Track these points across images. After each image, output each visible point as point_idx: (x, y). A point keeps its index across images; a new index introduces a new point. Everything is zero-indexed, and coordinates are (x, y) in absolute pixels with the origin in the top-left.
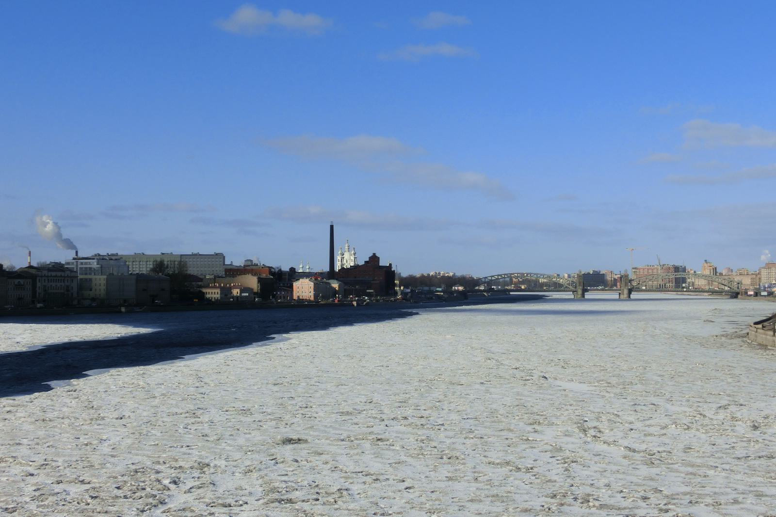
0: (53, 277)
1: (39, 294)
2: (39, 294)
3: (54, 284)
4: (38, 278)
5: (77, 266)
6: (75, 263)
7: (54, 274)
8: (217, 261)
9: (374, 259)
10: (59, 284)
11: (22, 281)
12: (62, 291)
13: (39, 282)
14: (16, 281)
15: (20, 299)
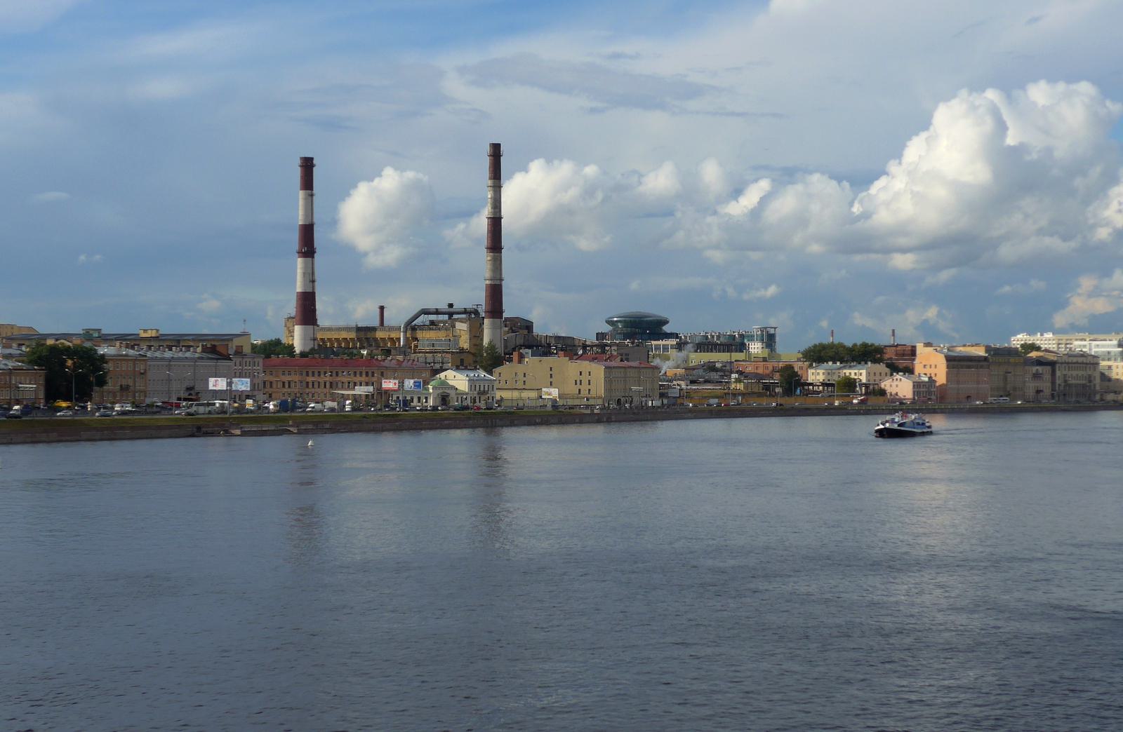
1: (1059, 385)
2: (1059, 385)
3: (1074, 373)
4: (1057, 366)
5: (1090, 349)
6: (1088, 347)
7: (1075, 360)
8: (1050, 344)
10: (1080, 373)
11: (1040, 369)
12: (1084, 382)
13: (1059, 370)
14: (1034, 369)
15: (1038, 392)
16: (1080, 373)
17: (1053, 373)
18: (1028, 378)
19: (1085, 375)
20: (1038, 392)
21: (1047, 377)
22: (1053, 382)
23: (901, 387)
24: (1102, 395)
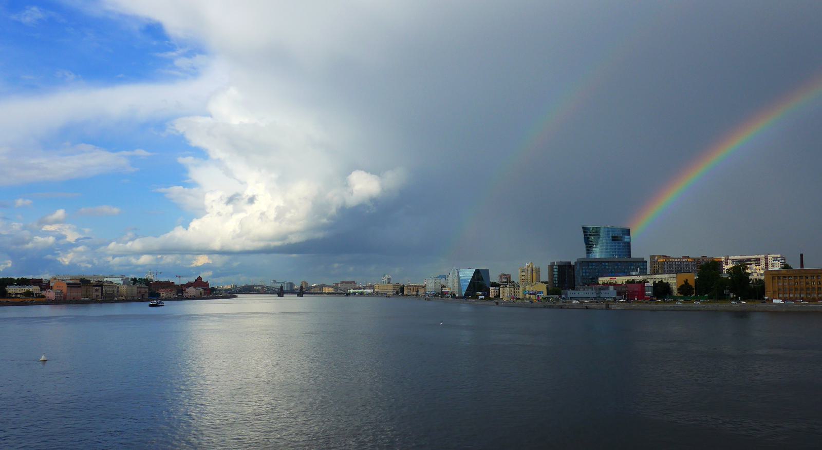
10: (111, 289)
14: (96, 288)
15: (97, 296)
16: (111, 289)
17: (102, 290)
18: (94, 290)
20: (97, 296)
21: (100, 291)
22: (102, 294)
23: (50, 294)
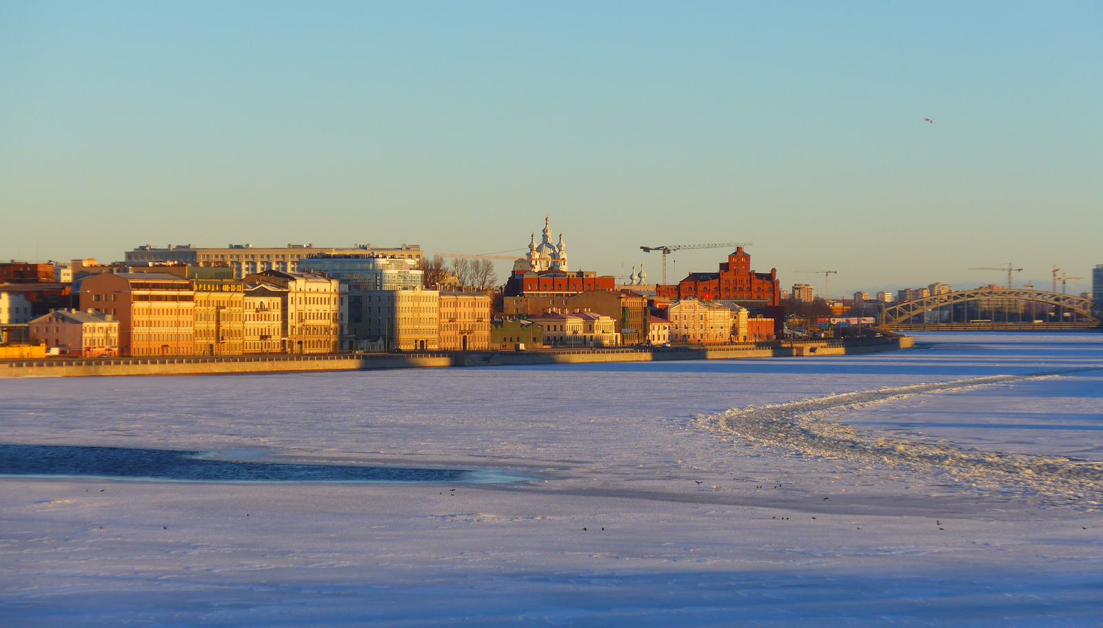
0: (314, 292)
3: (314, 308)
9: (740, 257)
13: (292, 303)
19: (328, 311)
21: (278, 312)
24: (351, 343)
